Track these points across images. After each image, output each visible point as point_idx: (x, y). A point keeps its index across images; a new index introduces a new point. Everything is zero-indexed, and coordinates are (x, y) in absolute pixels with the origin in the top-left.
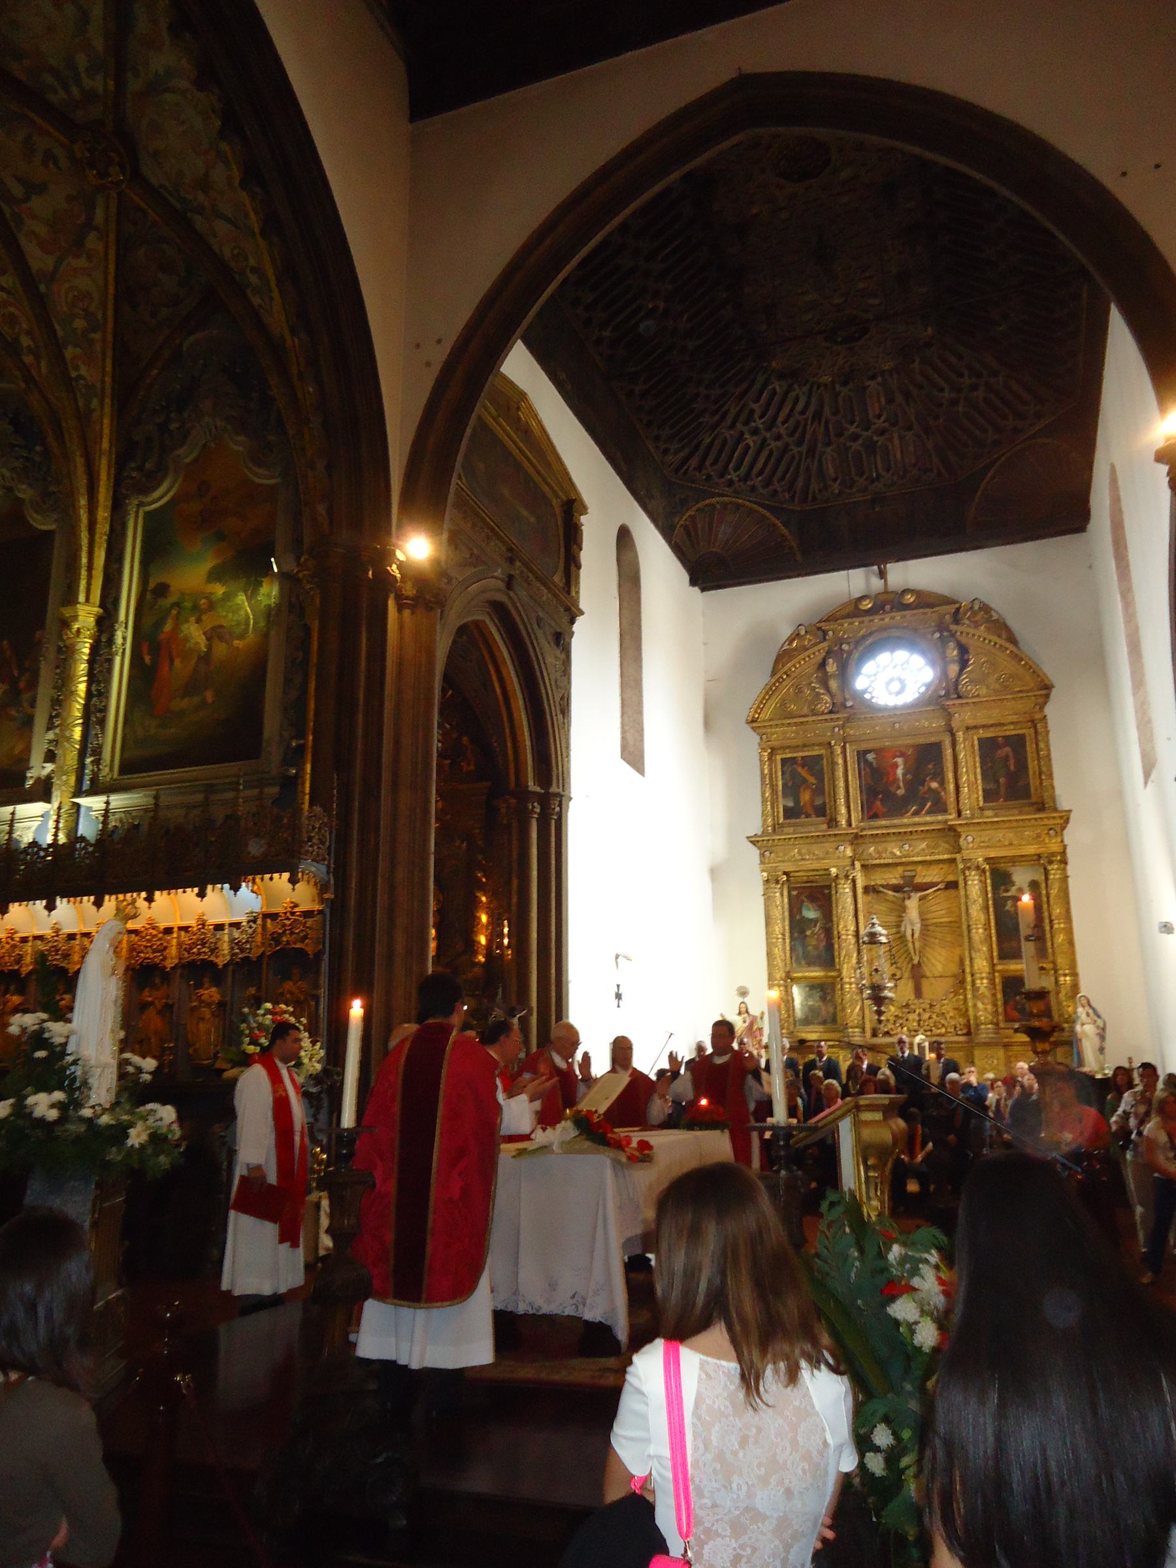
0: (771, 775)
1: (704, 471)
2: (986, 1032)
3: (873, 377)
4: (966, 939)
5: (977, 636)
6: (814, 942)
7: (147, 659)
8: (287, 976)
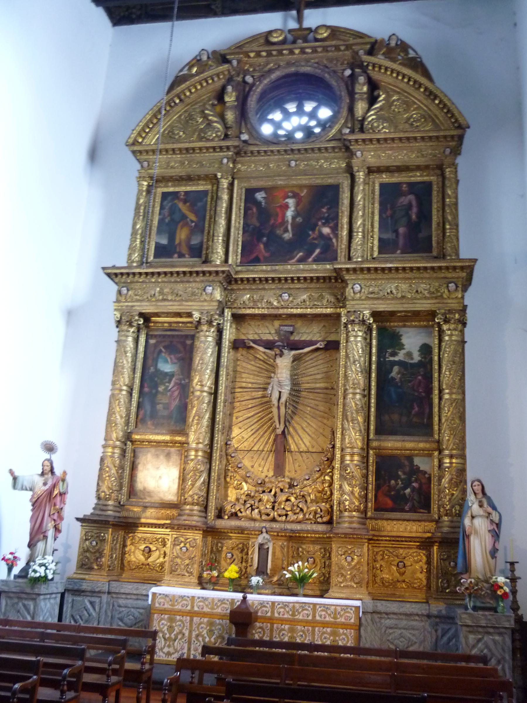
2: (349, 521)
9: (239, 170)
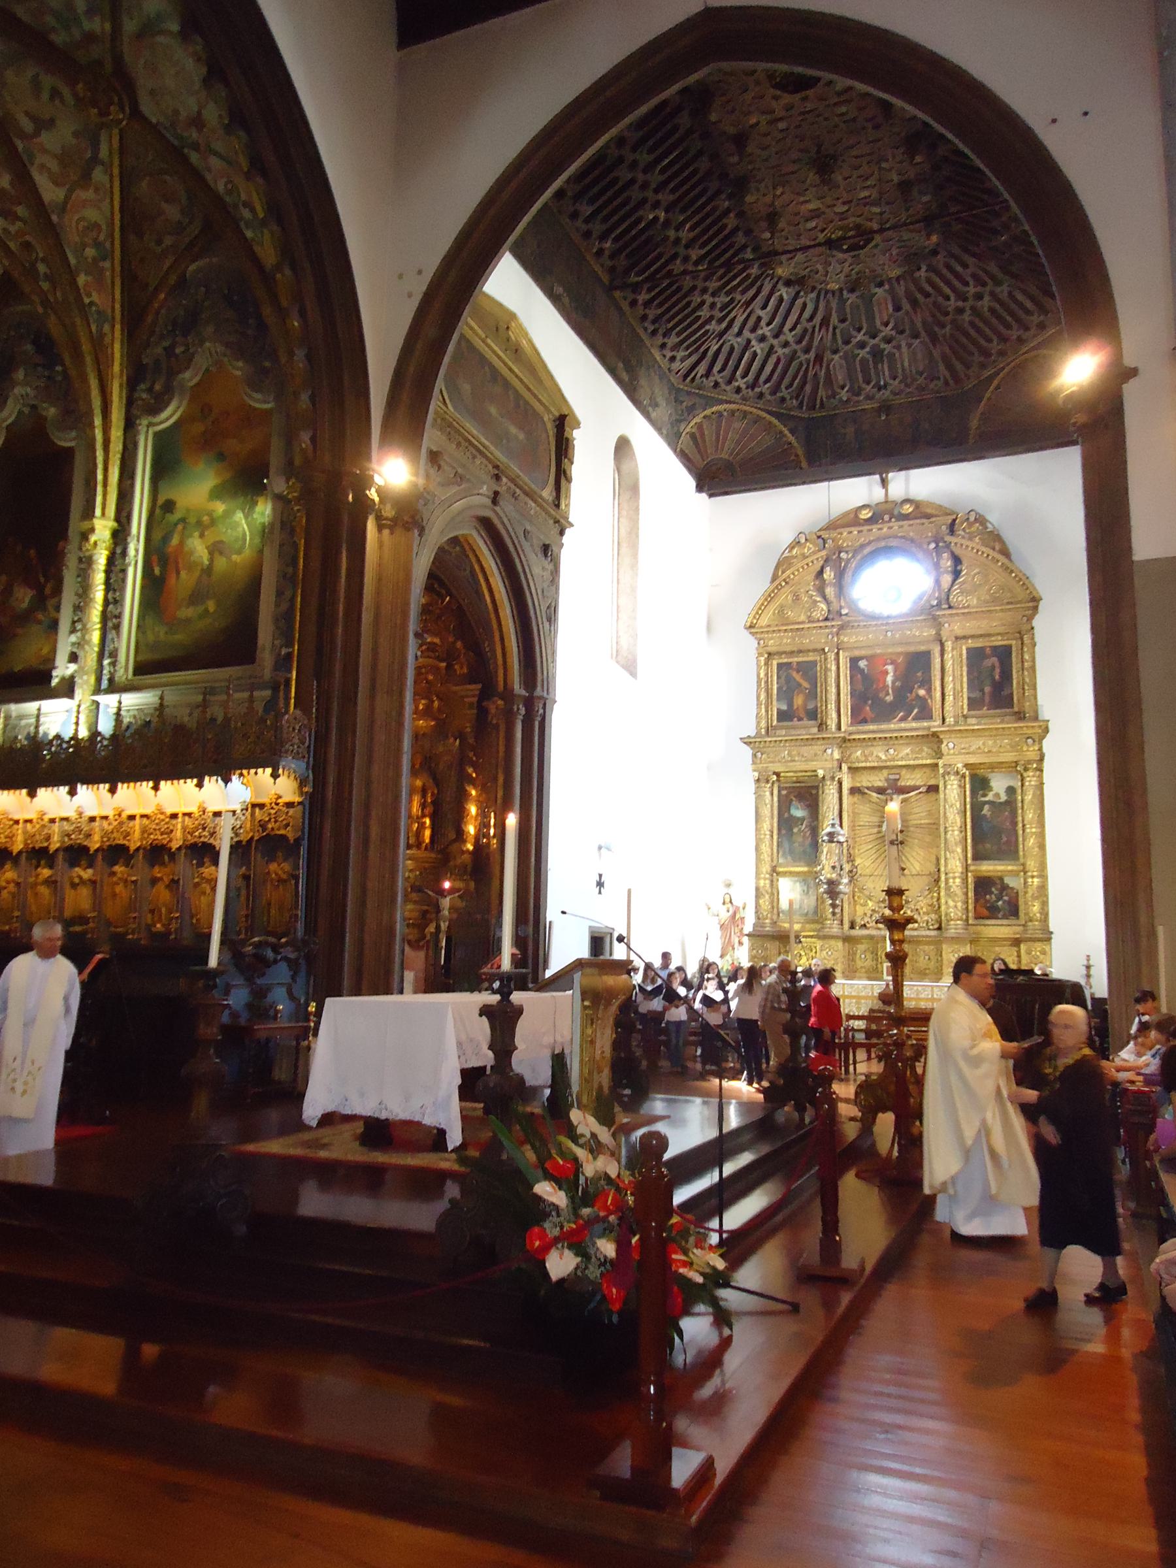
0: (767, 682)
1: (712, 378)
2: (955, 928)
3: (880, 285)
4: (943, 841)
5: (968, 546)
6: (800, 839)
7: (157, 571)
8: (272, 859)
9: (843, 642)
